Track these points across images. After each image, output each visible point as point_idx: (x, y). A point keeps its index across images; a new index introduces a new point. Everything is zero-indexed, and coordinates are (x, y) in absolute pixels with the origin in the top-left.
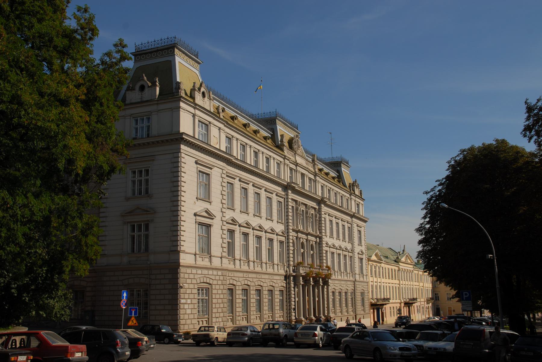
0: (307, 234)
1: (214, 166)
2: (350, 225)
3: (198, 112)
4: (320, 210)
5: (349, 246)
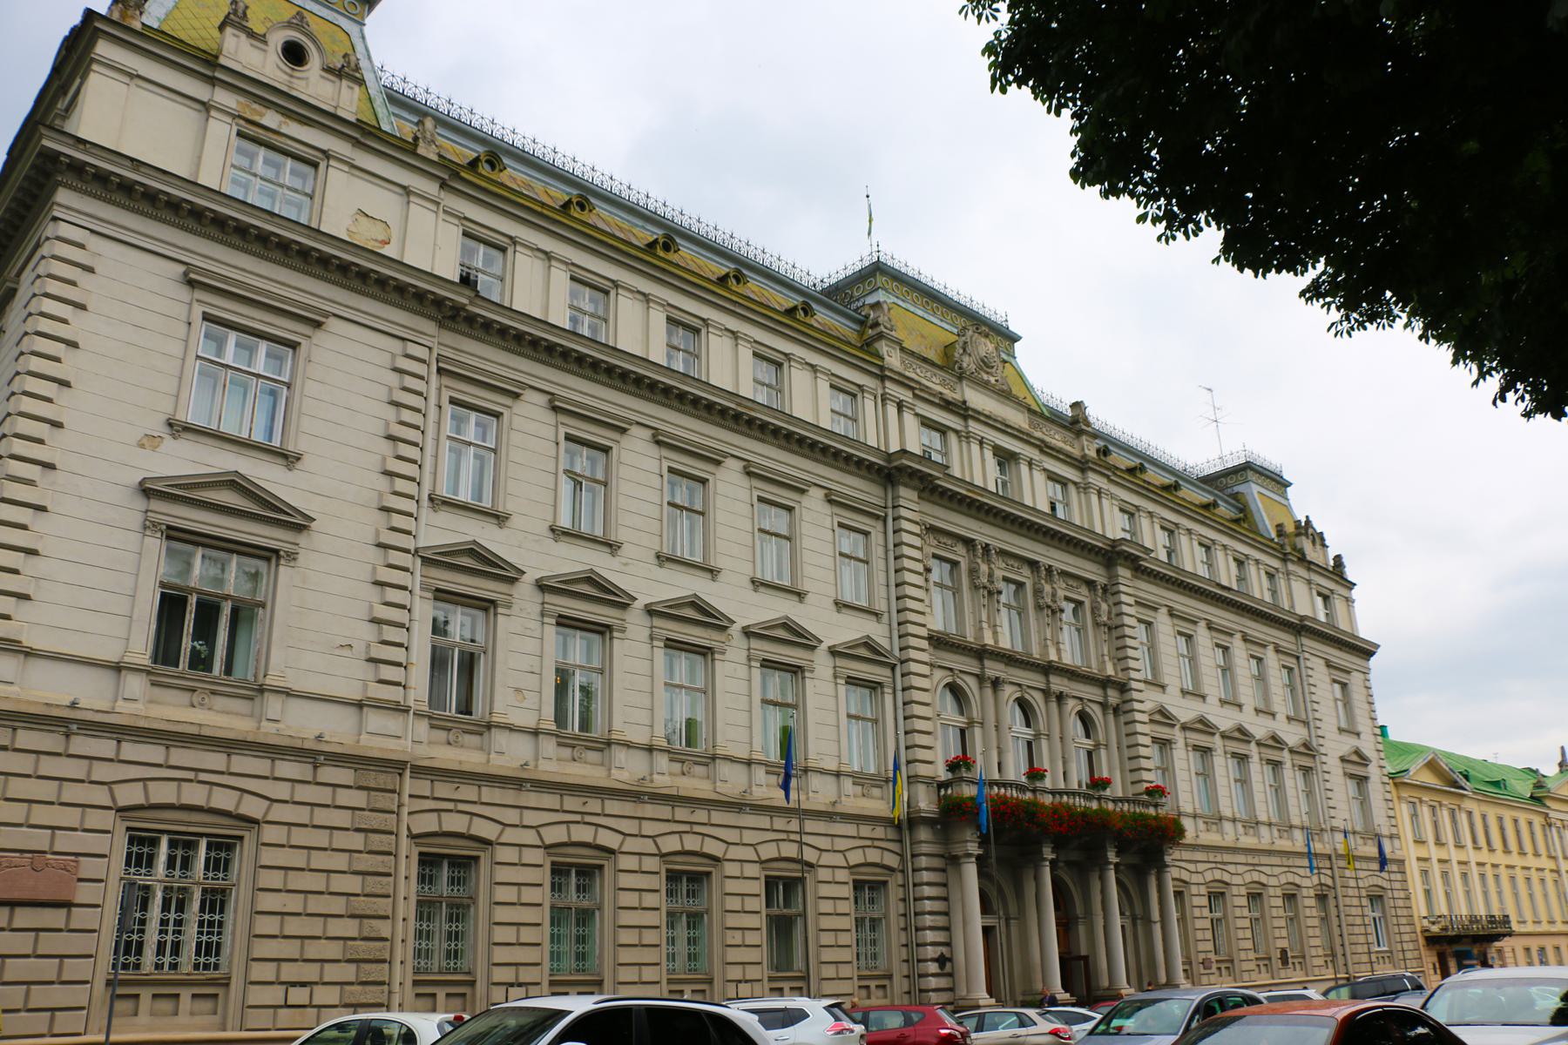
0: (1047, 669)
1: (327, 314)
2: (1294, 661)
4: (1109, 590)
5: (1293, 735)
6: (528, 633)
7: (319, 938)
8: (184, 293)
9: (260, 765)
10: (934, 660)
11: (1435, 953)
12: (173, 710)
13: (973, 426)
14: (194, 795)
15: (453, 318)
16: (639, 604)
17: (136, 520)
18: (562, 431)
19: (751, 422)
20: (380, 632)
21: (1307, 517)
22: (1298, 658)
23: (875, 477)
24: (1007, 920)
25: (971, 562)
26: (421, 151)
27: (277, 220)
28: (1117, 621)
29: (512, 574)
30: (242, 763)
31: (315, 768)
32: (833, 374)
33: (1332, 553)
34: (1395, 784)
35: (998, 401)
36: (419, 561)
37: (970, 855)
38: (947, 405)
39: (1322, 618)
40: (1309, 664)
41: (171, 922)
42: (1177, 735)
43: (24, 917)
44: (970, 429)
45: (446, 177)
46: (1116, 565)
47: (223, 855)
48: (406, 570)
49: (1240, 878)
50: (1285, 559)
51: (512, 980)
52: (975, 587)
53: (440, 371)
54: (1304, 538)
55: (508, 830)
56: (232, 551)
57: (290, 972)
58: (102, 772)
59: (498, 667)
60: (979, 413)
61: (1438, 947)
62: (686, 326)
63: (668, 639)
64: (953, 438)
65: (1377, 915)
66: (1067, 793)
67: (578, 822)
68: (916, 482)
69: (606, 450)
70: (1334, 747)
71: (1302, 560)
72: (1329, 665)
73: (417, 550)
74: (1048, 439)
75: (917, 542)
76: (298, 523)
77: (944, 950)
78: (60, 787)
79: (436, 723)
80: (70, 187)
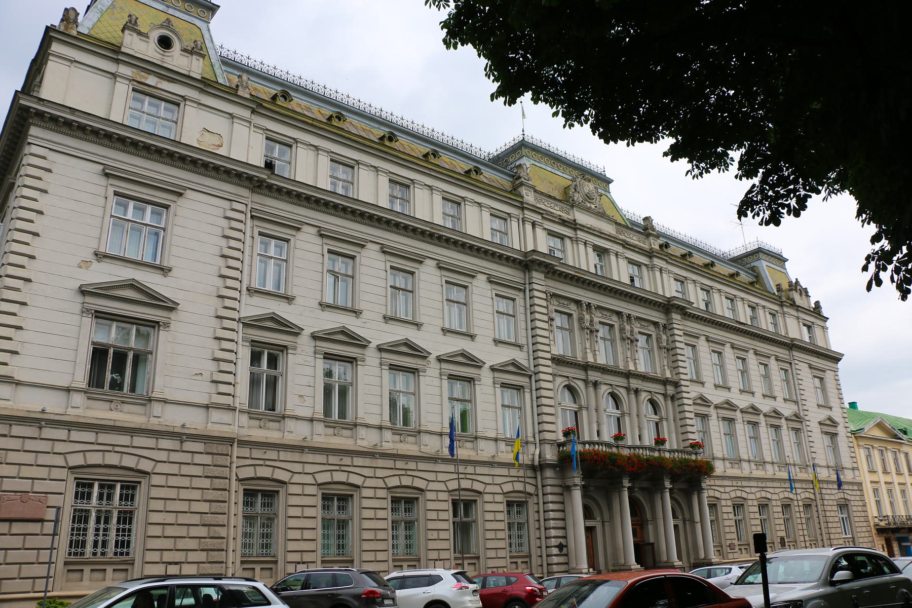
0: (628, 375)
2: (788, 365)
3: (124, 70)
5: (787, 410)
6: (307, 363)
7: (185, 537)
8: (103, 181)
9: (150, 442)
10: (556, 372)
11: (883, 539)
12: (100, 412)
13: (580, 234)
14: (112, 459)
15: (259, 187)
16: (373, 345)
17: (77, 308)
18: (326, 248)
19: (440, 238)
20: (219, 366)
21: (797, 279)
22: (791, 364)
23: (518, 267)
24: (603, 523)
25: (579, 314)
26: (240, 93)
27: (154, 137)
28: (672, 346)
29: (296, 331)
30: (139, 441)
31: (182, 442)
32: (491, 208)
33: (812, 301)
34: (855, 437)
35: (596, 218)
36: (241, 325)
37: (576, 485)
38: (564, 223)
39: (807, 340)
40: (797, 367)
41: (101, 530)
42: (712, 412)
43: (17, 528)
44: (578, 236)
45: (255, 107)
46: (671, 312)
47: (130, 492)
48: (233, 330)
49: (753, 495)
50: (782, 305)
51: (299, 560)
52: (582, 328)
53: (252, 217)
54: (794, 292)
55: (296, 475)
56: (133, 323)
57: (168, 557)
58: (60, 447)
59: (289, 384)
60: (584, 226)
61: (885, 535)
62: (401, 184)
63: (391, 365)
64: (568, 241)
65: (844, 516)
66: (642, 448)
67: (337, 470)
68: (543, 269)
69: (353, 258)
70: (815, 416)
71: (793, 305)
72: (811, 367)
73: (239, 319)
74: (628, 240)
75: (544, 303)
76: (170, 307)
77: (562, 540)
78: (37, 456)
79: (252, 416)
80: (37, 126)
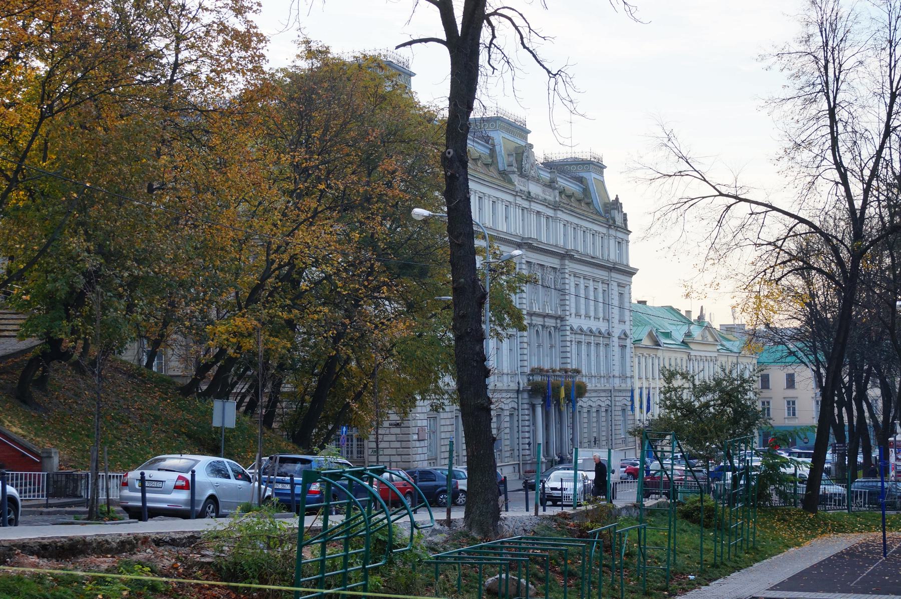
70: (616, 333)
